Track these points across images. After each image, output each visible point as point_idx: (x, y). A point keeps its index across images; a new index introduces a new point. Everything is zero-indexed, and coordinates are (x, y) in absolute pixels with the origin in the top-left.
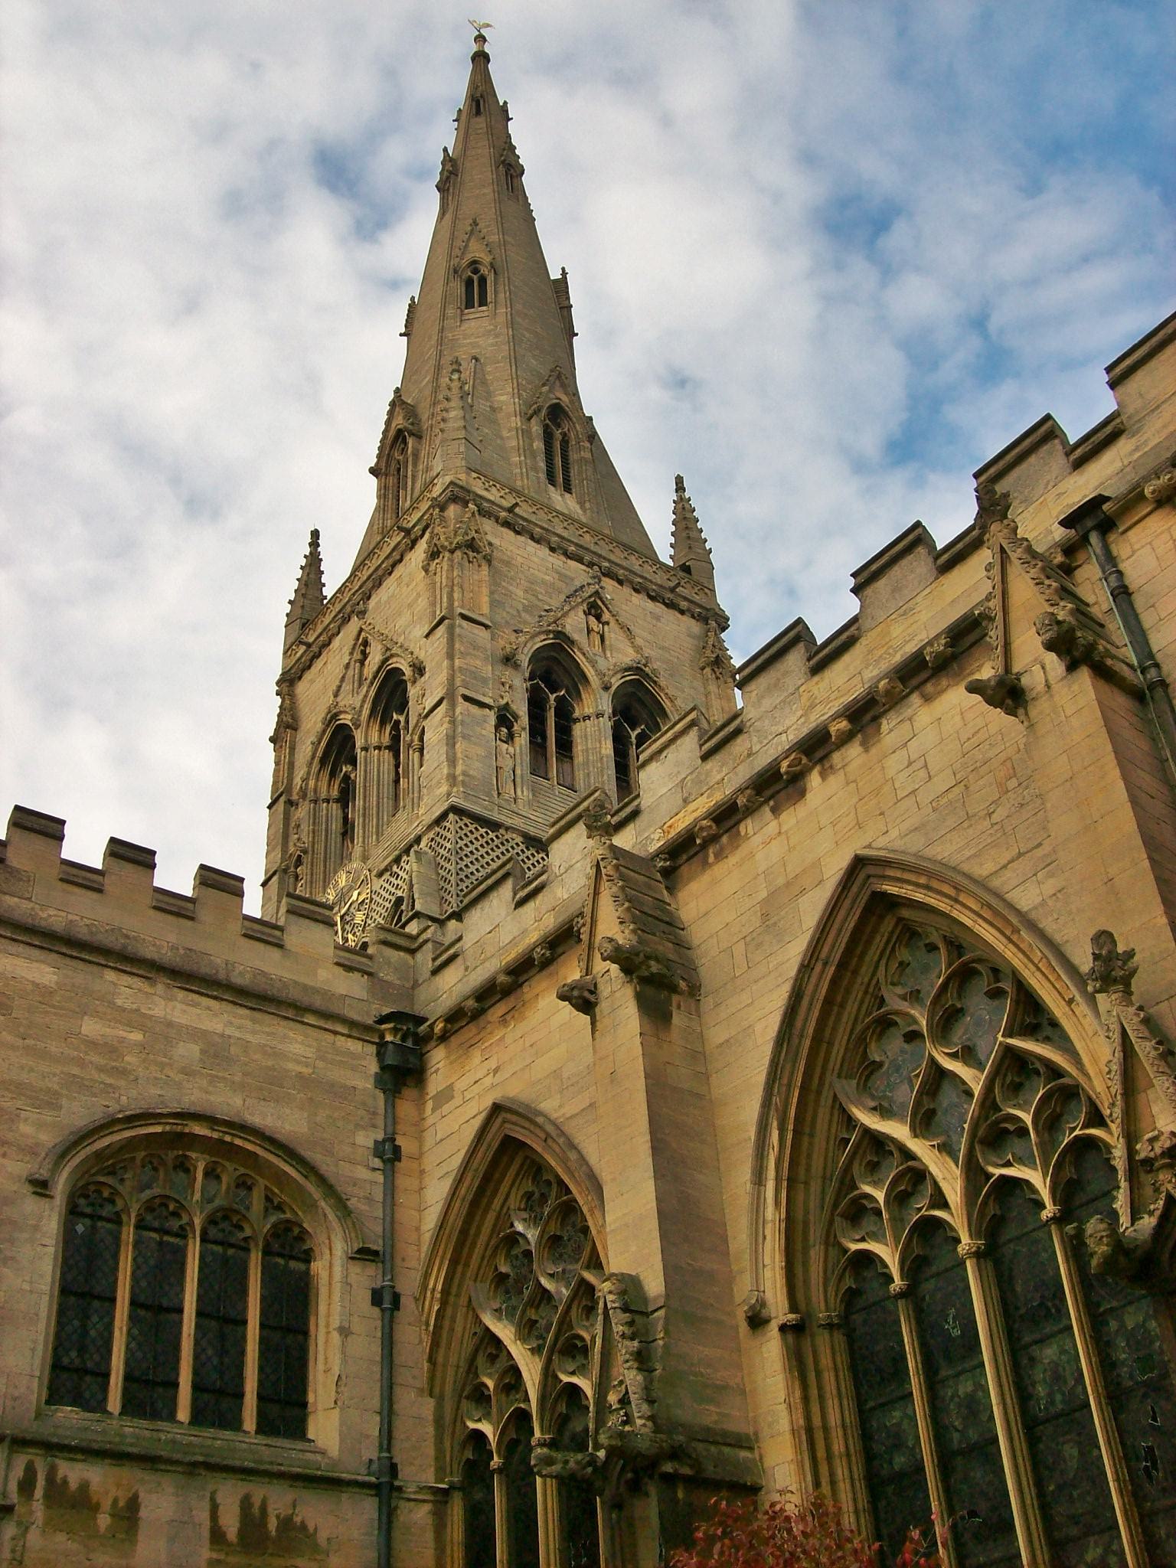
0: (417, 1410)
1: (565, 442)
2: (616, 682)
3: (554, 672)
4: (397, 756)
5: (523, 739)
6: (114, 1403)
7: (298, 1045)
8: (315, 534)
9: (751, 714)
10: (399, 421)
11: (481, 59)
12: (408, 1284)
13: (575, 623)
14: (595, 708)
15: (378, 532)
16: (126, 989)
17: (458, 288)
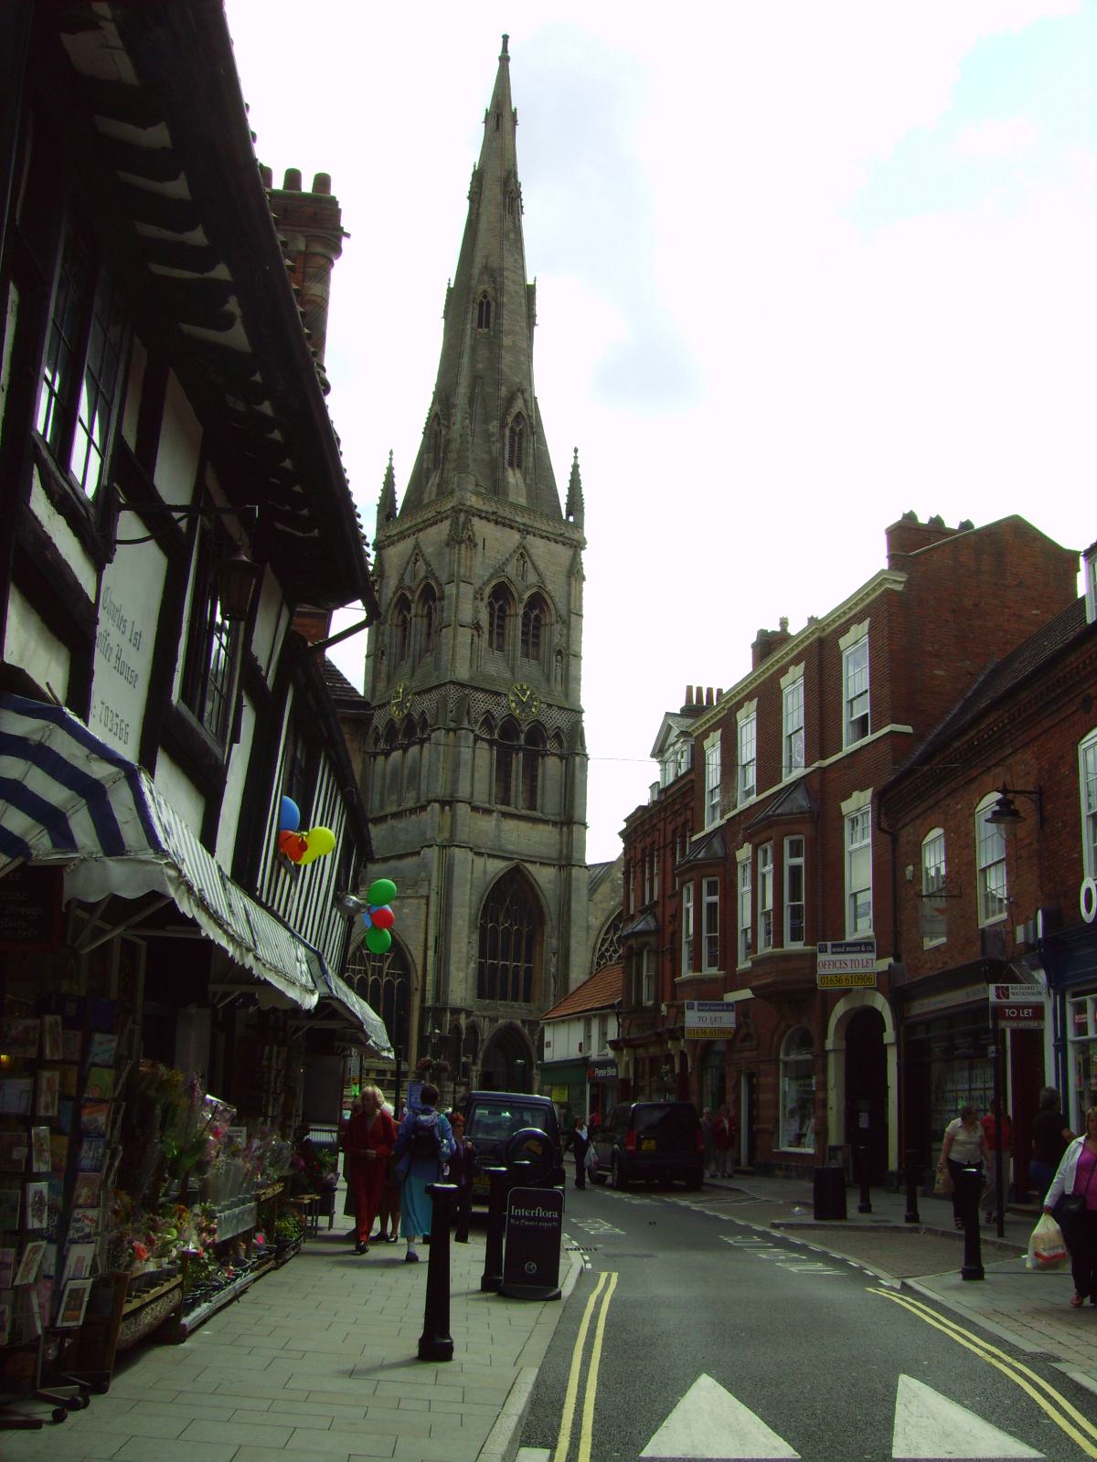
2: (526, 596)
3: (501, 594)
8: (391, 453)
11: (500, 119)
13: (511, 570)
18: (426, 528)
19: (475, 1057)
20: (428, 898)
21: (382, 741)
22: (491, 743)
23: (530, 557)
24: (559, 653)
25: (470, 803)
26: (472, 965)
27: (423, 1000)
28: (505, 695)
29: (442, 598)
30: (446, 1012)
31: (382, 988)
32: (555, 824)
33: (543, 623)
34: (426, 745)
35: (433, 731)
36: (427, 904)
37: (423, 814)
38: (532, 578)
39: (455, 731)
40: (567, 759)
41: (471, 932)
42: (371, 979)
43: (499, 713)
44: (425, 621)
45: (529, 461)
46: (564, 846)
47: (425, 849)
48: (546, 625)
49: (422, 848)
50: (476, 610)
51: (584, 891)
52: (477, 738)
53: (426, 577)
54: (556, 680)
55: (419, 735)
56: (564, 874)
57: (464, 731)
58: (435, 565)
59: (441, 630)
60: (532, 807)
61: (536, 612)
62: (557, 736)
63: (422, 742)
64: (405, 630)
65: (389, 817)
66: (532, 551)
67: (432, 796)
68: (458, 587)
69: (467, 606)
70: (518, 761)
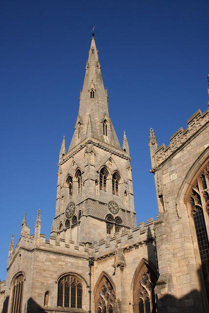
0: (93, 304)
1: (106, 126)
3: (103, 171)
4: (79, 182)
5: (99, 185)
6: (63, 306)
7: (80, 262)
9: (134, 236)
12: (92, 290)
13: (107, 164)
14: (110, 177)
16: (63, 257)
69: (92, 173)
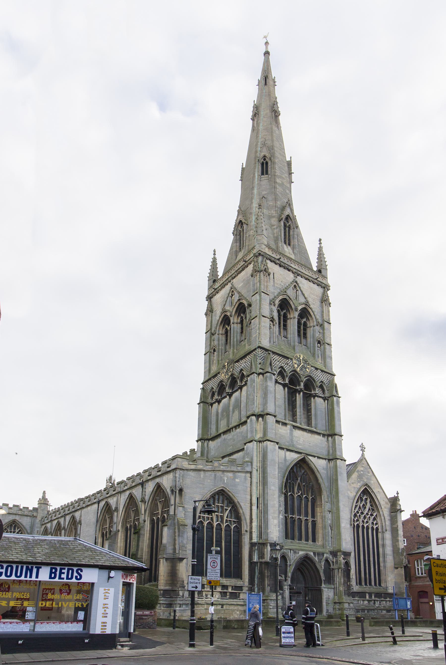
2: (300, 308)
10: (241, 217)
15: (233, 253)
17: (259, 168)
18: (238, 274)
19: (286, 577)
20: (251, 473)
21: (216, 394)
22: (284, 385)
23: (300, 288)
24: (319, 342)
25: (275, 416)
26: (281, 517)
27: (251, 538)
28: (291, 359)
29: (250, 305)
30: (267, 546)
31: (223, 530)
32: (324, 435)
33: (308, 326)
34: (244, 389)
35: (248, 376)
36: (251, 477)
37: (245, 427)
38: (302, 300)
39: (263, 374)
40: (328, 400)
41: (279, 496)
42: (215, 524)
43: (288, 369)
44: (239, 326)
45: (294, 242)
46: (331, 449)
47: (248, 444)
48: (310, 327)
49: (245, 444)
50: (271, 311)
51: (345, 475)
52: (276, 382)
53: (239, 300)
54: (318, 357)
55: (239, 383)
56: (332, 464)
57: (268, 374)
58: (243, 292)
59: (251, 322)
60: (309, 423)
61: (305, 320)
62: (321, 387)
63: (241, 388)
64: (227, 336)
65: (222, 435)
66: (300, 285)
67: (249, 413)
68: (260, 296)
69: (265, 308)
70: (299, 398)
